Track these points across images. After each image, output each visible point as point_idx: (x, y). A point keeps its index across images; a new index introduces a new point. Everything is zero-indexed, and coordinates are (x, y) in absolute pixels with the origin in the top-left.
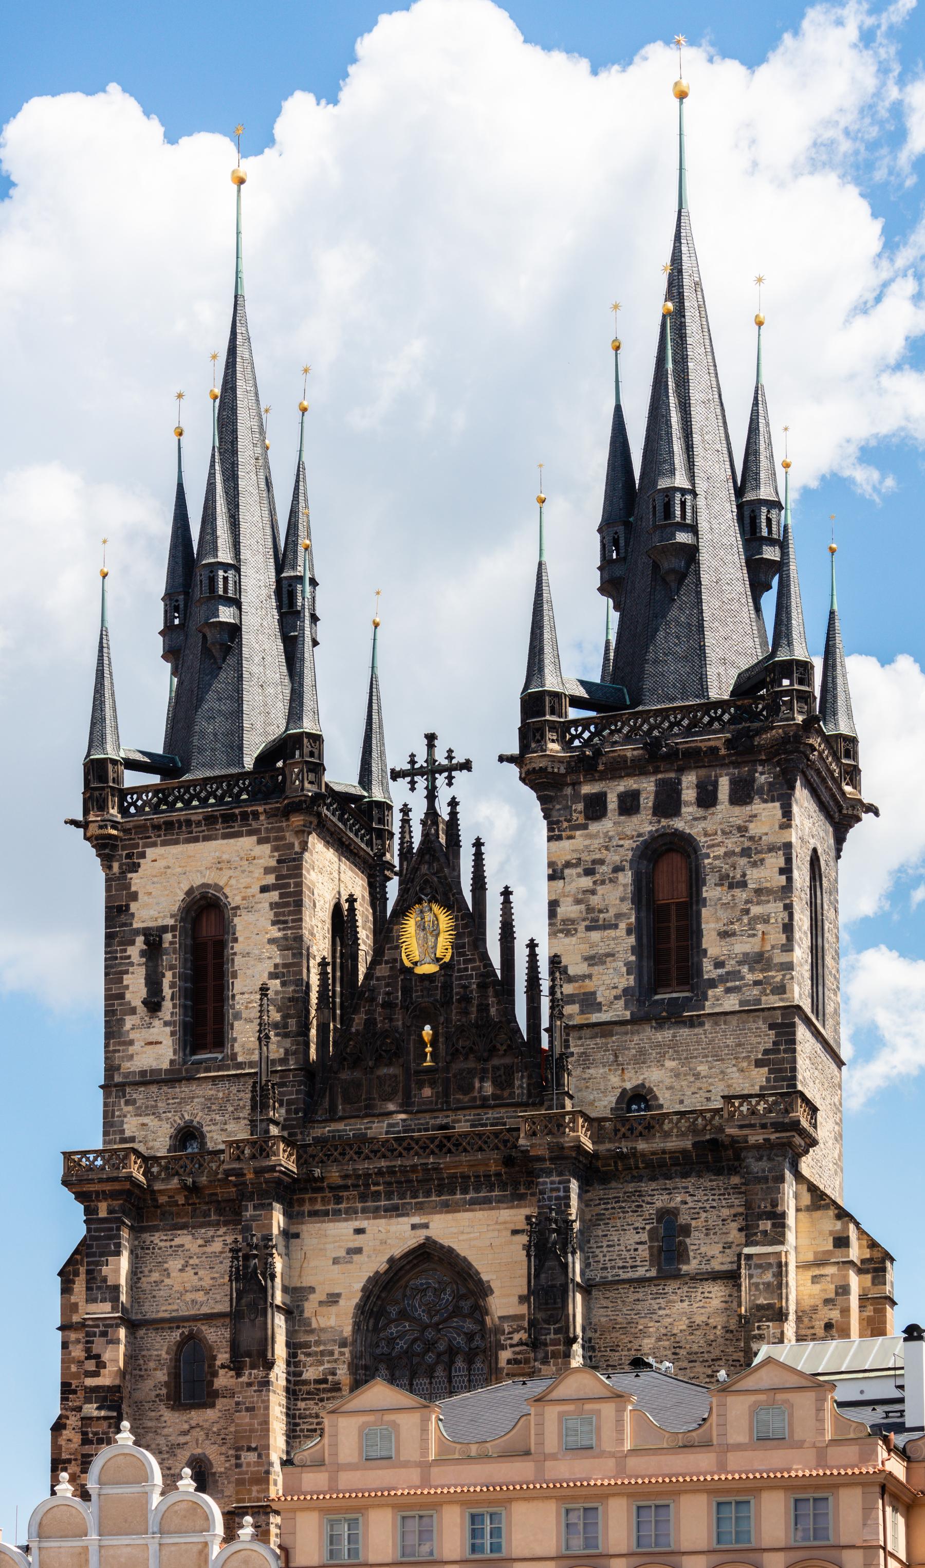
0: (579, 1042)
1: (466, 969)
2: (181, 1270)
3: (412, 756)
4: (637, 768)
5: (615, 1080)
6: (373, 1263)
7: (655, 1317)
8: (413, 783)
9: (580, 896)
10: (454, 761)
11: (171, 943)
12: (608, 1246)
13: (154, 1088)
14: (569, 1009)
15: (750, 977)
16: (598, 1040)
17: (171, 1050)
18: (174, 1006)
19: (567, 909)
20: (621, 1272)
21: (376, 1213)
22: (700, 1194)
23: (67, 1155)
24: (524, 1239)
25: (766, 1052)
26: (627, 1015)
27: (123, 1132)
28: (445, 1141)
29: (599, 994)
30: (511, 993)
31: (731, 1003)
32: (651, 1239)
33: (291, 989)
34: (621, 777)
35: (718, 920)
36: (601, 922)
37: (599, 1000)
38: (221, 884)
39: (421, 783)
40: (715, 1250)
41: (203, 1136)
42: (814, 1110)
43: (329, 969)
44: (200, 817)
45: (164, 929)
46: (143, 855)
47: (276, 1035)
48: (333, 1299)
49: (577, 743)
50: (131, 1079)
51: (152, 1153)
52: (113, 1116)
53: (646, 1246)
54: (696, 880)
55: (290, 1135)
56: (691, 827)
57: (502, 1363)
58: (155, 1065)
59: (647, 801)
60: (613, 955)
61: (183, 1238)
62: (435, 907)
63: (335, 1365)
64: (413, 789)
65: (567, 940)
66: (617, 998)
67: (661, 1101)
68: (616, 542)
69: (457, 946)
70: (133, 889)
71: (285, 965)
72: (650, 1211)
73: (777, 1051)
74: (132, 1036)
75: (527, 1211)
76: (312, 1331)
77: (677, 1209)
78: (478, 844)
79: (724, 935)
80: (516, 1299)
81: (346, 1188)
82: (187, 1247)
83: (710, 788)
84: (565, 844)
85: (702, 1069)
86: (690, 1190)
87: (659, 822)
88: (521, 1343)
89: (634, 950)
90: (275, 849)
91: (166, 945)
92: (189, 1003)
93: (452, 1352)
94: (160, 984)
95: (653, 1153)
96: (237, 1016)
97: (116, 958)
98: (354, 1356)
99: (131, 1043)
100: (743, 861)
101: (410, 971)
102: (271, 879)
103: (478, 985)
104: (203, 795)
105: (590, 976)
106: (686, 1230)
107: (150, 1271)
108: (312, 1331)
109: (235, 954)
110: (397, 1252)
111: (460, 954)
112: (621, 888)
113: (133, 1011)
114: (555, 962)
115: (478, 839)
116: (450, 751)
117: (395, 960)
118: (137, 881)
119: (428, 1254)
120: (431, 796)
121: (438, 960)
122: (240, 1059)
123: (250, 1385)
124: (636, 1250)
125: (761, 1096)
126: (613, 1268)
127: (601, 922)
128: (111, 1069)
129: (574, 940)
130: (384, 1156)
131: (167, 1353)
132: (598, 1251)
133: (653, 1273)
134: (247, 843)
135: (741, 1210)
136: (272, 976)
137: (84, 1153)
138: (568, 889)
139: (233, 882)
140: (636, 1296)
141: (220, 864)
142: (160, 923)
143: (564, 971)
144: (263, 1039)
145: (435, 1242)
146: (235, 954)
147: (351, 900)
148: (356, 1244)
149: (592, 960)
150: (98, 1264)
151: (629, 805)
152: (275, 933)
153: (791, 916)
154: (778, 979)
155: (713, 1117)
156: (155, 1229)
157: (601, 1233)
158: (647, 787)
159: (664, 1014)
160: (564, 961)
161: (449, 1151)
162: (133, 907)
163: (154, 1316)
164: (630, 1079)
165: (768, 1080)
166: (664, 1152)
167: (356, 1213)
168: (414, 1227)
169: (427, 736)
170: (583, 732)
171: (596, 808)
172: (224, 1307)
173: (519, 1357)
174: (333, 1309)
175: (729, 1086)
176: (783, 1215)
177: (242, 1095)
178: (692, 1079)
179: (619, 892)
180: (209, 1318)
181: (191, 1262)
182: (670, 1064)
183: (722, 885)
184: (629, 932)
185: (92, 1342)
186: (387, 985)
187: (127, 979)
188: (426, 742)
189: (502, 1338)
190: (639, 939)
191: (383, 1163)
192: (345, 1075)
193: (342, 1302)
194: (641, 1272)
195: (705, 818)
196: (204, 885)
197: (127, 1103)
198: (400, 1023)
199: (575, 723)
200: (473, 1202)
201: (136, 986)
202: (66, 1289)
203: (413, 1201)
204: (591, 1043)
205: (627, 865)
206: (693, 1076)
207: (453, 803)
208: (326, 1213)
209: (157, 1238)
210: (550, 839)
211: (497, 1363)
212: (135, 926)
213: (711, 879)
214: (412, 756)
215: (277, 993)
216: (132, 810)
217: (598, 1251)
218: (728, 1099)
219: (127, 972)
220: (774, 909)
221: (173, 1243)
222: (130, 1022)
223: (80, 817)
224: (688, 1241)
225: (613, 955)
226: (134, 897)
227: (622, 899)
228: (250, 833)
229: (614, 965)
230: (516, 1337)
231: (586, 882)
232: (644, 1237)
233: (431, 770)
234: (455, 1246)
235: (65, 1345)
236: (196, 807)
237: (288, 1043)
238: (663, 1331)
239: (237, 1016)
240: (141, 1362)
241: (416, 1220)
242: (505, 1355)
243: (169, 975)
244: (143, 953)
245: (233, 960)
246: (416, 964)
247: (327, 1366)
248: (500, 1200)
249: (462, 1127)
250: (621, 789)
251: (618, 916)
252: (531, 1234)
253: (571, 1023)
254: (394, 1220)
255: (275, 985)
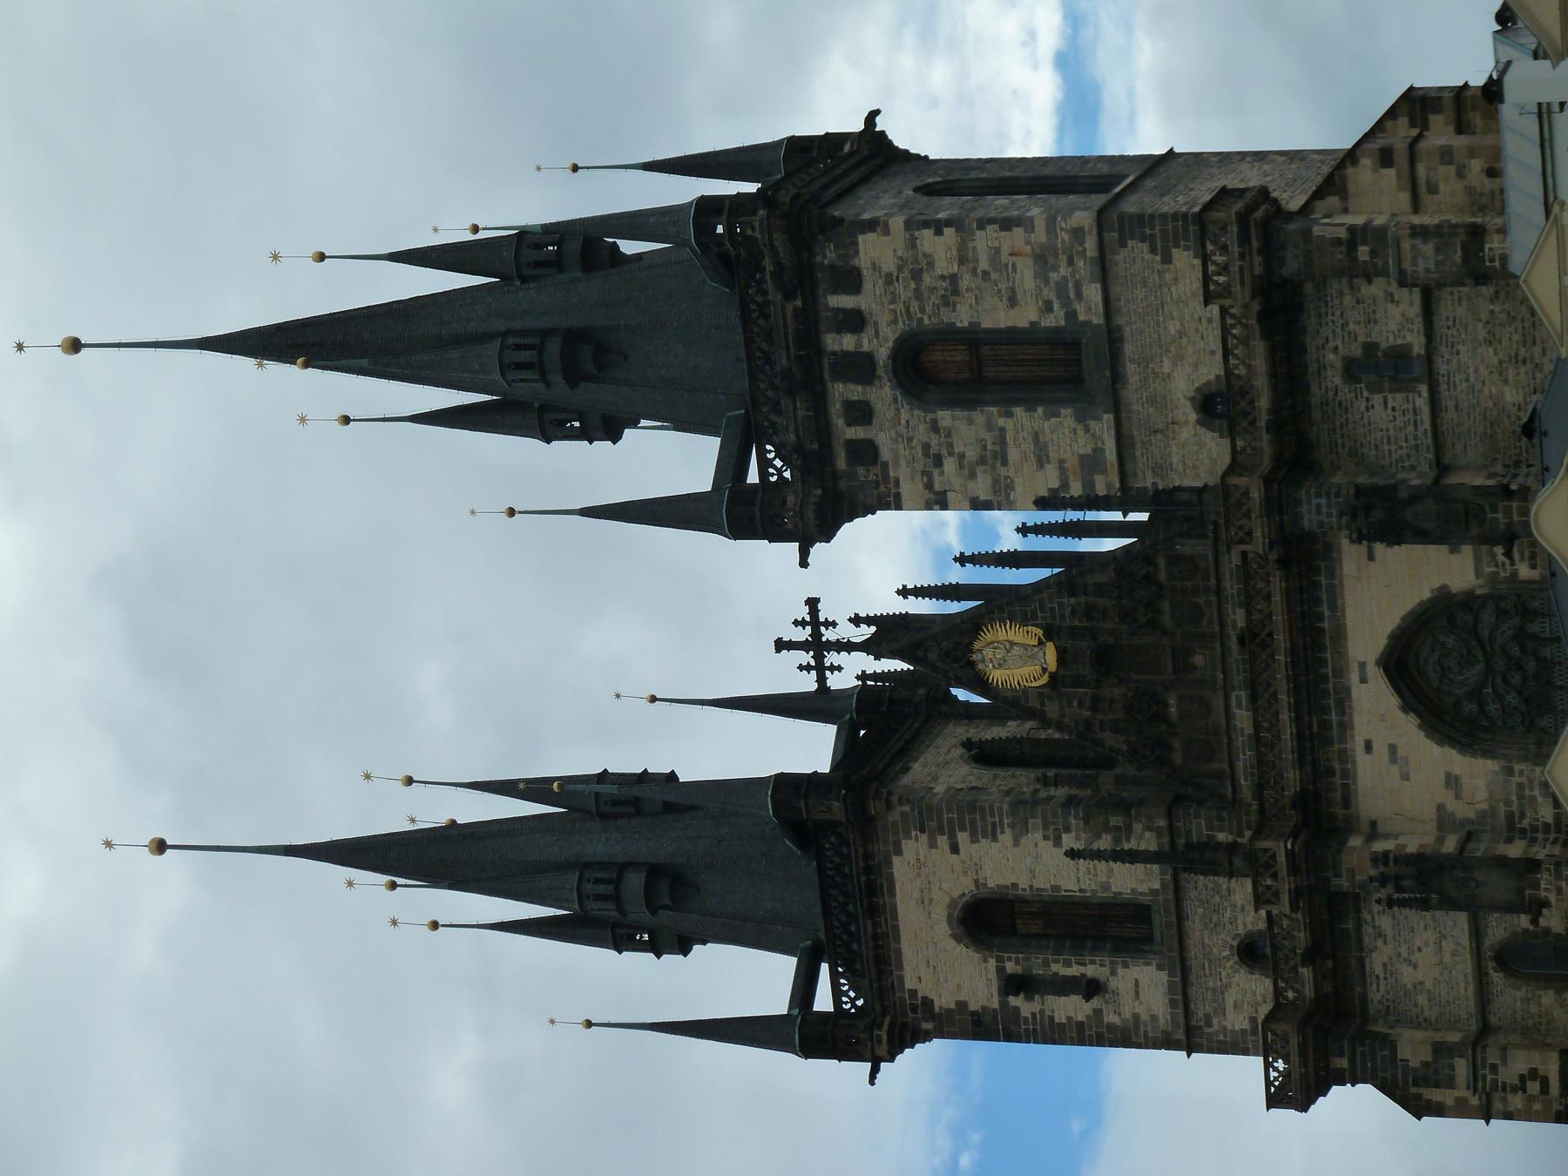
0: (1140, 475)
1: (1052, 609)
2: (1415, 967)
3: (801, 668)
4: (819, 402)
5: (1185, 433)
6: (1407, 731)
7: (1478, 386)
8: (833, 668)
9: (966, 471)
10: (808, 619)
11: (1017, 963)
12: (1389, 443)
13: (1192, 991)
14: (1101, 490)
15: (1064, 270)
16: (1138, 453)
17: (1146, 968)
18: (1093, 962)
19: (981, 488)
20: (1421, 428)
21: (1345, 726)
22: (1326, 331)
23: (1273, 1101)
24: (1379, 548)
25: (1153, 250)
26: (1108, 417)
27: (1244, 1032)
28: (1258, 640)
29: (1082, 451)
30: (1081, 557)
31: (1093, 293)
32: (1380, 390)
33: (1073, 822)
34: (828, 423)
35: (995, 308)
36: (997, 448)
37: (1089, 451)
38: (947, 900)
39: (832, 658)
40: (1395, 312)
41: (1249, 934)
42: (1224, 192)
43: (1051, 773)
44: (869, 923)
45: (1000, 970)
46: (913, 993)
47: (1128, 840)
48: (1452, 782)
49: (787, 474)
50: (1182, 1020)
51: (1270, 997)
52: (1225, 1042)
53: (1389, 396)
54: (950, 335)
55: (1249, 828)
56: (886, 339)
57: (1534, 574)
58: (1163, 989)
59: (856, 392)
60: (1036, 434)
61: (1376, 962)
62: (977, 645)
63: (1536, 782)
64: (839, 668)
65: (1019, 489)
66: (1087, 430)
67: (1212, 377)
68: (562, 423)
69: (1025, 622)
70: (952, 1006)
71: (1045, 828)
72: (1345, 393)
73: (1152, 237)
74: (1127, 1015)
75: (1345, 543)
76: (1493, 810)
77: (1344, 359)
78: (904, 592)
79: (1013, 301)
80: (1453, 556)
81: (1314, 763)
82: (1385, 960)
83: (840, 317)
84: (905, 489)
85: (1173, 327)
86: (1320, 342)
87: (880, 378)
88: (1508, 554)
89: (1030, 408)
90: (908, 836)
91: (1019, 970)
92: (1089, 945)
93: (1521, 636)
94: (1066, 979)
95: (1274, 387)
96: (1106, 887)
97: (1034, 1030)
98: (1525, 759)
99: (1136, 1017)
100: (927, 279)
101: (1053, 676)
102: (943, 841)
103: (1072, 595)
104: (844, 918)
105: (1061, 462)
106: (1370, 348)
107: (1416, 1005)
108: (1493, 810)
109: (1031, 887)
110: (1392, 701)
111: (1034, 617)
112: (957, 423)
113: (1098, 1012)
114: (1042, 504)
115: (899, 592)
116: (796, 623)
117: (1041, 695)
118: (944, 1000)
119: (1400, 664)
120: (848, 647)
121: (1041, 643)
122: (1157, 886)
123: (1559, 891)
124: (1394, 409)
125: (1206, 260)
126: (1416, 437)
127: (997, 448)
128: (1166, 1042)
129: (1018, 482)
130: (1277, 713)
131: (1519, 989)
132: (1395, 456)
133: (1424, 389)
134: (900, 868)
135: (1345, 281)
136: (1057, 842)
137: (1268, 1083)
138: (958, 488)
139: (945, 886)
140: (1451, 409)
141: (925, 902)
142: (993, 975)
143: (1053, 491)
144: (1132, 857)
145: (1382, 655)
146: (1031, 887)
147: (968, 744)
148: (1385, 750)
149: (1041, 460)
150: (1406, 1069)
151: (861, 413)
152: (1006, 837)
153: (991, 221)
154: (1066, 236)
155: (1233, 316)
156: (1364, 996)
157: (1373, 452)
158: (841, 392)
159: (1108, 373)
160: (1044, 493)
161: (1270, 635)
162: (972, 1007)
163: (1472, 1003)
164: (1186, 414)
165: (1187, 248)
166: (1273, 375)
167: (1345, 750)
168: (1363, 680)
169: (778, 650)
170: (775, 467)
171: (865, 452)
172: (1462, 918)
173: (1527, 554)
174: (1465, 781)
175: (1194, 295)
176: (1352, 229)
177: (1200, 884)
178: (1185, 340)
179: (962, 427)
180: (1477, 934)
181: (1405, 954)
182: (1166, 368)
183: (954, 304)
184: (1009, 415)
185: (1504, 1084)
186: (1070, 704)
187: (1060, 1018)
188: (784, 652)
189: (1503, 574)
190: (1017, 402)
191: (1285, 716)
192: (1178, 758)
193: (1456, 771)
194: (1422, 402)
195: (876, 323)
196: (949, 921)
197: (1209, 1024)
198: (1115, 690)
199: (763, 474)
200: (1333, 607)
201: (1069, 1008)
202: (1438, 1111)
203: (1332, 680)
204: (1141, 461)
205: (930, 416)
206: (1182, 337)
207: (856, 620)
208: (1346, 787)
209: (1376, 995)
210: (899, 507)
211: (1535, 582)
212: (996, 1005)
213: (946, 316)
214: (801, 668)
215: (1078, 838)
216: (860, 1003)
217: (1395, 456)
218: (1208, 299)
219: (1051, 1018)
220: (983, 241)
221: (1382, 976)
222: (1111, 1018)
223: (866, 1067)
224: (1384, 346)
225: (1036, 434)
226: (962, 1005)
227: (970, 422)
228: (889, 864)
229: (1047, 432)
230: (1501, 558)
231: (950, 465)
232: (1377, 399)
233: (817, 646)
234: (1389, 630)
235: (1508, 1116)
236: (858, 928)
237: (1138, 827)
238: (1495, 376)
239: (1106, 887)
240: (1530, 1022)
241: (1354, 677)
242: (1525, 572)
243: (1055, 968)
244: (1029, 998)
245: (1039, 890)
246: (1045, 670)
247: (1537, 792)
248: (1331, 574)
249: (1238, 618)
250: (841, 422)
251: (990, 426)
252: (1372, 539)
253: (1117, 486)
254: (1355, 704)
255: (1069, 841)
